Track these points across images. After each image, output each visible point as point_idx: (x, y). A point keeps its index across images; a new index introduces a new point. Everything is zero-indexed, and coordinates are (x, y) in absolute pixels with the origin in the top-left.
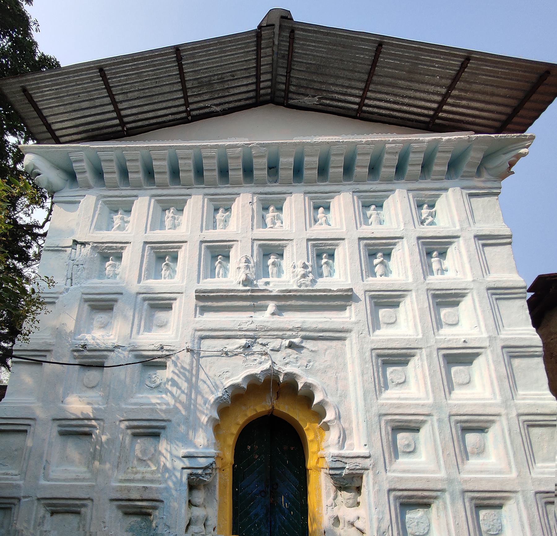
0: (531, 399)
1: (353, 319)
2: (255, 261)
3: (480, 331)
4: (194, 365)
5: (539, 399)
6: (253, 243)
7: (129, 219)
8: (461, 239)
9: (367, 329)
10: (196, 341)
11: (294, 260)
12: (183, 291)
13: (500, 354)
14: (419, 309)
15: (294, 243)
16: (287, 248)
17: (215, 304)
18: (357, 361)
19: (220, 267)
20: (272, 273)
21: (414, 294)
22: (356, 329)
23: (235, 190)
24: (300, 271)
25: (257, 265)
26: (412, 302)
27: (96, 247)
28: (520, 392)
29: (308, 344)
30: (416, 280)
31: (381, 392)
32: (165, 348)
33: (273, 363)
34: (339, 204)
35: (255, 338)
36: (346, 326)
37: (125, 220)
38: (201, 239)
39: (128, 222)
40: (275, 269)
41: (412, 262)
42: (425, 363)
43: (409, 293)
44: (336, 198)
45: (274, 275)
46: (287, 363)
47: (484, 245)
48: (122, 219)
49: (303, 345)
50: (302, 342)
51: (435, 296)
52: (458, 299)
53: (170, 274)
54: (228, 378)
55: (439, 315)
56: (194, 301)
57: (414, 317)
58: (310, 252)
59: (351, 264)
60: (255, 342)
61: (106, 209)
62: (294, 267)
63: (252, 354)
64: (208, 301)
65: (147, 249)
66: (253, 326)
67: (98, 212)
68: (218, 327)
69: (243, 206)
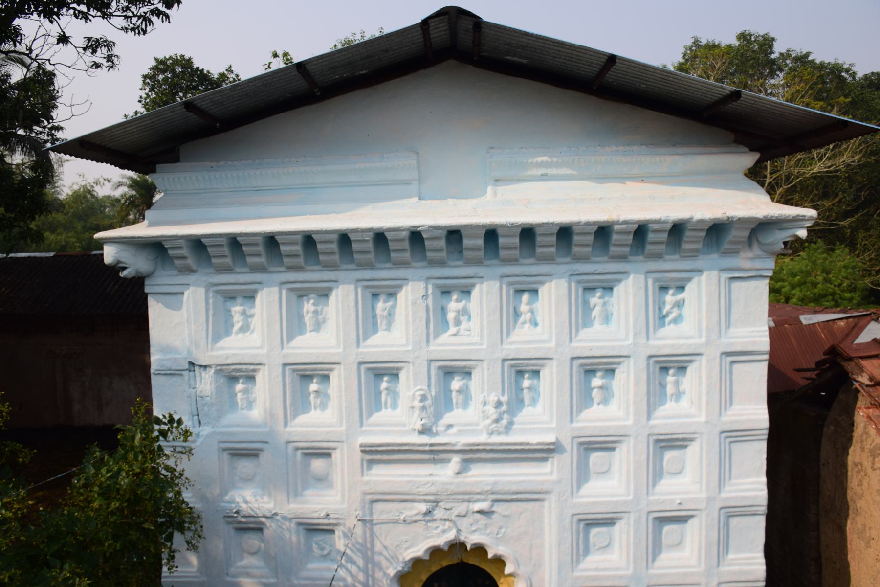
1: (555, 477)
2: (433, 394)
4: (368, 535)
7: (252, 311)
8: (704, 357)
9: (569, 490)
10: (367, 506)
12: (344, 438)
15: (485, 365)
17: (385, 457)
19: (388, 394)
20: (457, 403)
21: (632, 441)
25: (436, 399)
27: (220, 370)
29: (499, 508)
31: (578, 561)
32: (332, 516)
33: (459, 531)
35: (437, 502)
36: (545, 487)
37: (248, 313)
38: (361, 360)
39: (252, 316)
40: (461, 397)
42: (632, 529)
43: (627, 438)
44: (547, 285)
46: (474, 531)
48: (244, 313)
49: (494, 509)
50: (492, 506)
51: (658, 441)
52: (686, 443)
53: (321, 403)
54: (407, 549)
55: (662, 459)
56: (358, 455)
58: (506, 378)
60: (437, 506)
62: (485, 404)
63: (435, 520)
64: (375, 454)
65: (287, 373)
66: (433, 489)
67: (211, 312)
68: (392, 489)
69: (414, 303)
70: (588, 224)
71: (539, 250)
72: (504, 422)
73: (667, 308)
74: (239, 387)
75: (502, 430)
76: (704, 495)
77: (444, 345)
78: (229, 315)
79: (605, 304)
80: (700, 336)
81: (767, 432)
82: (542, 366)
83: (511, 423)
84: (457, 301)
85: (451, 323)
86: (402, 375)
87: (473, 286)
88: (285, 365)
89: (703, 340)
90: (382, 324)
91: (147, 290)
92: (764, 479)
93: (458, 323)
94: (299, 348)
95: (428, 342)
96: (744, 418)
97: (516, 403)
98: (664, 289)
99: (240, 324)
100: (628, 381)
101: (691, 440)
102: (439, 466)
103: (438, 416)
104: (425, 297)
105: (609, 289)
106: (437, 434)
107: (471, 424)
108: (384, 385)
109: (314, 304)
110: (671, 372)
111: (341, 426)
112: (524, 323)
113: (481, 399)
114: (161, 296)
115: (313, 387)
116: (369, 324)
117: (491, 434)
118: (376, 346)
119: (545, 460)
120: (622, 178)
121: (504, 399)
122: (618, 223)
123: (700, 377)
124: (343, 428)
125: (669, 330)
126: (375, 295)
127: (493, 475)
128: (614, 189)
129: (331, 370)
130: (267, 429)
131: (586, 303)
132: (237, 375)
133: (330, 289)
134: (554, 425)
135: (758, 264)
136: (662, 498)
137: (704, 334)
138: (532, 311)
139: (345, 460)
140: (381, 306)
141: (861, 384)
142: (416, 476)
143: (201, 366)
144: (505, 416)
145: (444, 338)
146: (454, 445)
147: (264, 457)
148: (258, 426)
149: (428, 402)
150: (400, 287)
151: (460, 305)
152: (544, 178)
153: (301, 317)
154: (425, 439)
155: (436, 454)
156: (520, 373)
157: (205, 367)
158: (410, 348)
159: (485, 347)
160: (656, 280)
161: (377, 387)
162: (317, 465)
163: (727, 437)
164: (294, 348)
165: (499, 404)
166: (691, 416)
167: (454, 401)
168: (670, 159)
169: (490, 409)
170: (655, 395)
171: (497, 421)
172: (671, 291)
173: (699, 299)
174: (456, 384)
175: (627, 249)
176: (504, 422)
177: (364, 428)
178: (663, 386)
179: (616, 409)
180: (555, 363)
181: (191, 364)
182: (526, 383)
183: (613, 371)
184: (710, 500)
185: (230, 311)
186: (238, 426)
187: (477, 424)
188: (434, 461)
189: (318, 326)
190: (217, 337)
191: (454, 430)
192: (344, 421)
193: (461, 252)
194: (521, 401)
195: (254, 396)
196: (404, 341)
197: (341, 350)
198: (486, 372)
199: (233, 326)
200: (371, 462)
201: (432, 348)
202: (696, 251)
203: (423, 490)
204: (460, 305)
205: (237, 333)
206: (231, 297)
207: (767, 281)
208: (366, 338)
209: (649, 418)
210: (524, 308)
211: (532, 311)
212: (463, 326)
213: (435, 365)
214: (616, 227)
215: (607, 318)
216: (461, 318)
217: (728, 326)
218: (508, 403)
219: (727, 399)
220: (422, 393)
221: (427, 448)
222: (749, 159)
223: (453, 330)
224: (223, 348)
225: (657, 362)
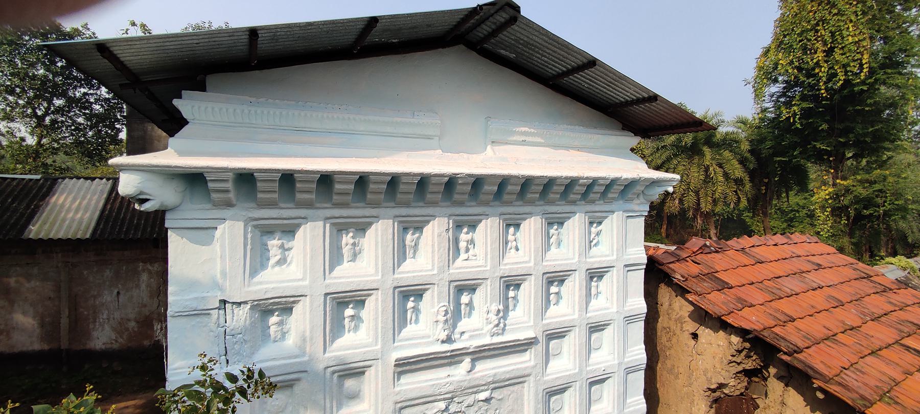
1: (532, 363)
7: (290, 244)
12: (379, 356)
14: (580, 345)
15: (489, 282)
17: (414, 367)
18: (532, 403)
23: (430, 211)
24: (493, 318)
25: (453, 312)
29: (496, 394)
30: (580, 315)
34: (530, 229)
36: (526, 372)
37: (286, 247)
38: (396, 284)
39: (289, 249)
41: (580, 297)
48: (282, 247)
56: (391, 368)
61: (258, 233)
64: (405, 366)
66: (451, 388)
67: (249, 247)
68: (419, 395)
69: (439, 235)
70: (566, 178)
72: (502, 325)
73: (593, 236)
75: (500, 332)
76: (616, 362)
77: (460, 268)
78: (265, 249)
82: (524, 280)
83: (505, 325)
85: (462, 250)
87: (480, 221)
89: (615, 257)
90: (410, 253)
91: (166, 225)
92: (644, 347)
93: (467, 250)
94: (340, 278)
99: (278, 257)
101: (608, 325)
102: (452, 367)
103: (454, 326)
105: (561, 224)
106: (455, 341)
109: (353, 237)
113: (485, 309)
114: (186, 231)
119: (526, 350)
122: (582, 178)
124: (379, 347)
126: (406, 229)
127: (493, 369)
128: (561, 154)
130: (306, 358)
136: (595, 367)
137: (615, 253)
142: (437, 379)
143: (234, 303)
144: (502, 321)
145: (459, 262)
146: (468, 348)
149: (449, 316)
151: (469, 236)
152: (524, 143)
153: (340, 248)
154: (446, 347)
155: (453, 358)
156: (508, 287)
157: (239, 304)
159: (488, 268)
161: (405, 306)
165: (499, 311)
166: (608, 309)
167: (463, 312)
171: (497, 325)
174: (465, 299)
176: (502, 325)
177: (396, 344)
180: (533, 277)
181: (224, 302)
184: (620, 364)
185: (266, 245)
186: (274, 359)
188: (450, 364)
189: (354, 256)
190: (254, 272)
191: (465, 336)
192: (380, 340)
195: (288, 326)
197: (380, 277)
198: (489, 287)
199: (268, 259)
200: (400, 374)
201: (451, 271)
202: (613, 199)
203: (443, 390)
204: (469, 236)
205: (273, 267)
206: (268, 231)
210: (510, 237)
212: (471, 252)
214: (581, 181)
215: (559, 244)
219: (624, 295)
220: (445, 308)
221: (449, 354)
222: (634, 141)
223: (463, 256)
224: (261, 283)
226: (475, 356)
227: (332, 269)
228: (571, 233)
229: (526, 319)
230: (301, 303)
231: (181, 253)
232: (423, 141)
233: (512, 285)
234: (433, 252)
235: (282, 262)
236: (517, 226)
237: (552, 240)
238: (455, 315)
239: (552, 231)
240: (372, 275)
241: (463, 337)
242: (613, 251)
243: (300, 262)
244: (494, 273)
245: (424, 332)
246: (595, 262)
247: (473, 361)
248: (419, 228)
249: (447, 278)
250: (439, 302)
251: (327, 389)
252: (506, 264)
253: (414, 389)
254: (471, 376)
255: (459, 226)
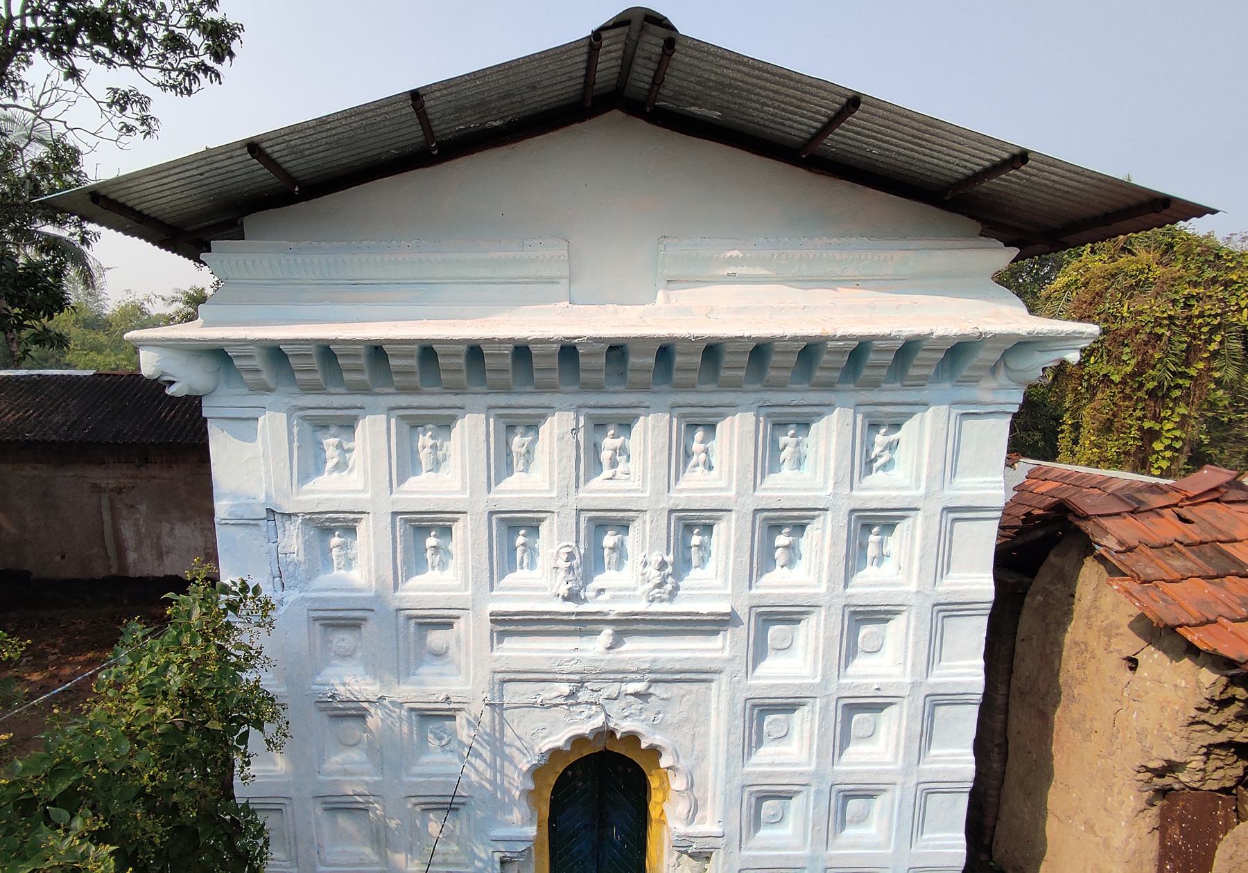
0: (943, 762)
1: (726, 654)
2: (582, 551)
3: (904, 672)
4: (497, 722)
5: (953, 762)
6: (578, 517)
11: (644, 546)
12: (470, 606)
13: (921, 703)
14: (826, 638)
15: (648, 516)
16: (636, 524)
17: (521, 628)
18: (724, 716)
19: (524, 551)
21: (823, 612)
22: (728, 670)
24: (654, 574)
25: (585, 558)
26: (818, 624)
28: (933, 752)
29: (656, 690)
30: (830, 590)
33: (607, 716)
34: (732, 433)
35: (582, 682)
36: (714, 666)
37: (346, 446)
38: (491, 508)
39: (350, 450)
40: (615, 555)
41: (832, 556)
45: (612, 566)
47: (955, 520)
48: (339, 446)
49: (651, 691)
50: (649, 687)
51: (854, 613)
54: (544, 738)
57: (816, 648)
59: (735, 559)
61: (307, 427)
63: (580, 704)
64: (508, 625)
66: (579, 667)
68: (528, 667)
69: (561, 438)
70: (794, 339)
71: (724, 373)
72: (669, 587)
73: (877, 450)
74: (335, 540)
75: (665, 596)
76: (908, 680)
77: (597, 491)
79: (798, 444)
80: (918, 487)
81: (990, 606)
82: (718, 519)
83: (676, 588)
84: (614, 436)
85: (606, 464)
86: (543, 528)
87: (637, 417)
88: (395, 514)
89: (922, 491)
90: (518, 463)
92: (981, 662)
93: (614, 464)
95: (577, 487)
96: (966, 587)
97: (683, 565)
98: (874, 426)
99: (335, 460)
100: (821, 542)
101: (897, 613)
102: (585, 639)
103: (587, 579)
104: (575, 430)
106: (585, 600)
107: (626, 589)
108: (520, 540)
110: (875, 530)
111: (466, 590)
112: (697, 465)
114: (229, 422)
115: (431, 541)
116: (503, 464)
117: (652, 601)
118: (511, 491)
119: (716, 633)
120: (832, 282)
121: (670, 558)
122: (833, 338)
123: (913, 537)
124: (469, 593)
125: (877, 477)
126: (511, 428)
127: (652, 651)
129: (455, 520)
131: (775, 442)
132: (332, 526)
133: (454, 418)
134: (729, 591)
135: (1001, 397)
136: (857, 681)
137: (923, 485)
138: (706, 451)
139: (471, 631)
140: (518, 442)
141: (1107, 549)
142: (557, 651)
144: (670, 580)
145: (597, 482)
147: (367, 629)
148: (360, 590)
149: (576, 562)
150: (543, 417)
151: (618, 442)
153: (415, 452)
154: (570, 607)
155: (584, 625)
156: (689, 528)
157: (290, 515)
158: (554, 494)
159: (647, 495)
160: (866, 415)
161: (511, 542)
162: (436, 638)
163: (940, 611)
164: (406, 492)
165: (663, 565)
168: (898, 255)
169: (652, 572)
170: (855, 558)
171: (659, 586)
172: (883, 430)
173: (921, 440)
174: (609, 540)
175: (837, 374)
176: (669, 587)
177: (494, 593)
178: (863, 547)
179: (807, 572)
180: (734, 515)
182: (695, 540)
183: (803, 527)
184: (914, 685)
185: (321, 443)
187: (635, 589)
188: (581, 634)
189: (437, 465)
190: (304, 478)
193: (623, 374)
194: (688, 562)
196: (546, 486)
197: (467, 496)
198: (648, 525)
200: (502, 635)
201: (581, 495)
202: (925, 378)
203: (567, 667)
204: (618, 442)
205: (330, 472)
206: (321, 425)
207: (1009, 419)
208: (498, 482)
209: (846, 586)
210: (696, 446)
211: (706, 451)
212: (621, 467)
213: (584, 516)
214: (830, 344)
215: (799, 462)
216: (618, 458)
217: (954, 475)
218: (673, 564)
219: (944, 564)
220: (569, 550)
221: (573, 618)
223: (607, 473)
224: (312, 492)
225: (859, 517)
226: (620, 628)
227: (401, 481)
228: (822, 443)
229: (719, 582)
230: (363, 522)
231: (224, 450)
232: (538, 286)
233: (697, 526)
234: (551, 464)
235: (341, 466)
236: (711, 428)
237: (783, 455)
238: (588, 564)
239: (783, 440)
240: (456, 492)
241: (600, 598)
242: (918, 479)
243: (360, 469)
244: (657, 502)
245: (538, 583)
246: (872, 499)
247: (616, 633)
248: (532, 427)
249: (572, 503)
250: (560, 540)
251: (401, 636)
252: (681, 491)
253: (521, 658)
254: (612, 655)
255: (599, 425)
